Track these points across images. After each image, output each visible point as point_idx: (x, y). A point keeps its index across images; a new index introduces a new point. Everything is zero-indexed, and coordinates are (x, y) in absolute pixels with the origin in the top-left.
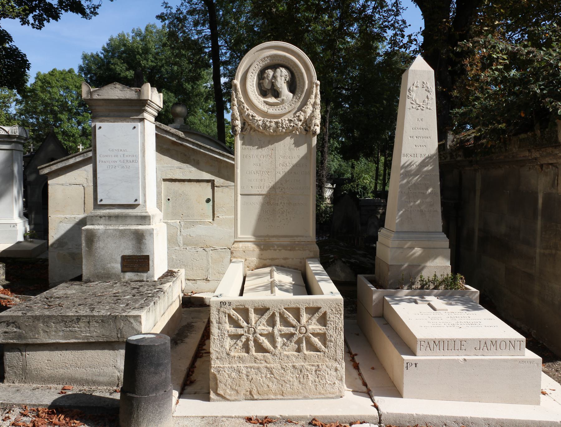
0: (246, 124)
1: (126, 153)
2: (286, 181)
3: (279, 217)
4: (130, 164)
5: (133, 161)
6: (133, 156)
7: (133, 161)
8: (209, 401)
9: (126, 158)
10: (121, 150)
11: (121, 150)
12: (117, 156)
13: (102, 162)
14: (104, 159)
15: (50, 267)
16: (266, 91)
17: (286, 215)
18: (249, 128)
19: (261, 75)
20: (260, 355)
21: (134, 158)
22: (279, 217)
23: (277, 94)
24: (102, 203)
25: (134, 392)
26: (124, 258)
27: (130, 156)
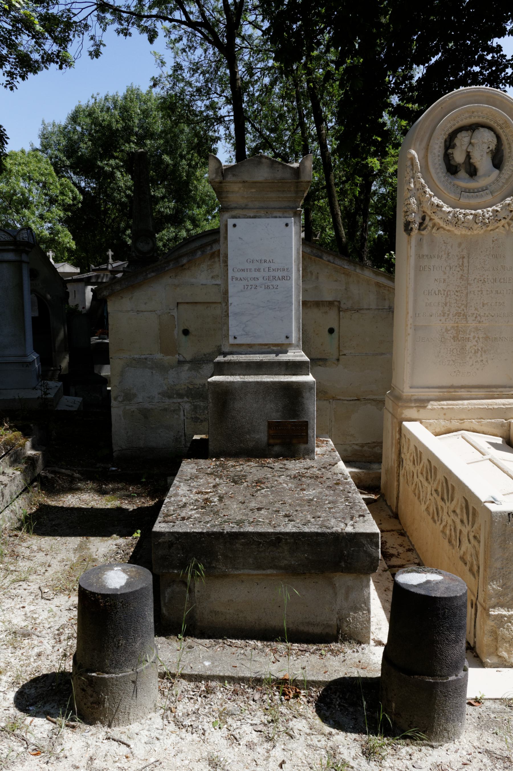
0: (427, 218)
1: (273, 266)
2: (483, 305)
3: (470, 358)
4: (278, 282)
5: (283, 278)
6: (284, 270)
7: (283, 278)
8: (484, 667)
9: (272, 274)
10: (265, 261)
11: (265, 261)
12: (259, 270)
13: (237, 279)
14: (239, 275)
15: (113, 429)
16: (456, 167)
17: (481, 356)
18: (431, 224)
19: (450, 143)
20: (468, 573)
21: (285, 274)
22: (470, 358)
23: (472, 172)
24: (237, 342)
25: (432, 675)
26: (271, 425)
27: (278, 269)
